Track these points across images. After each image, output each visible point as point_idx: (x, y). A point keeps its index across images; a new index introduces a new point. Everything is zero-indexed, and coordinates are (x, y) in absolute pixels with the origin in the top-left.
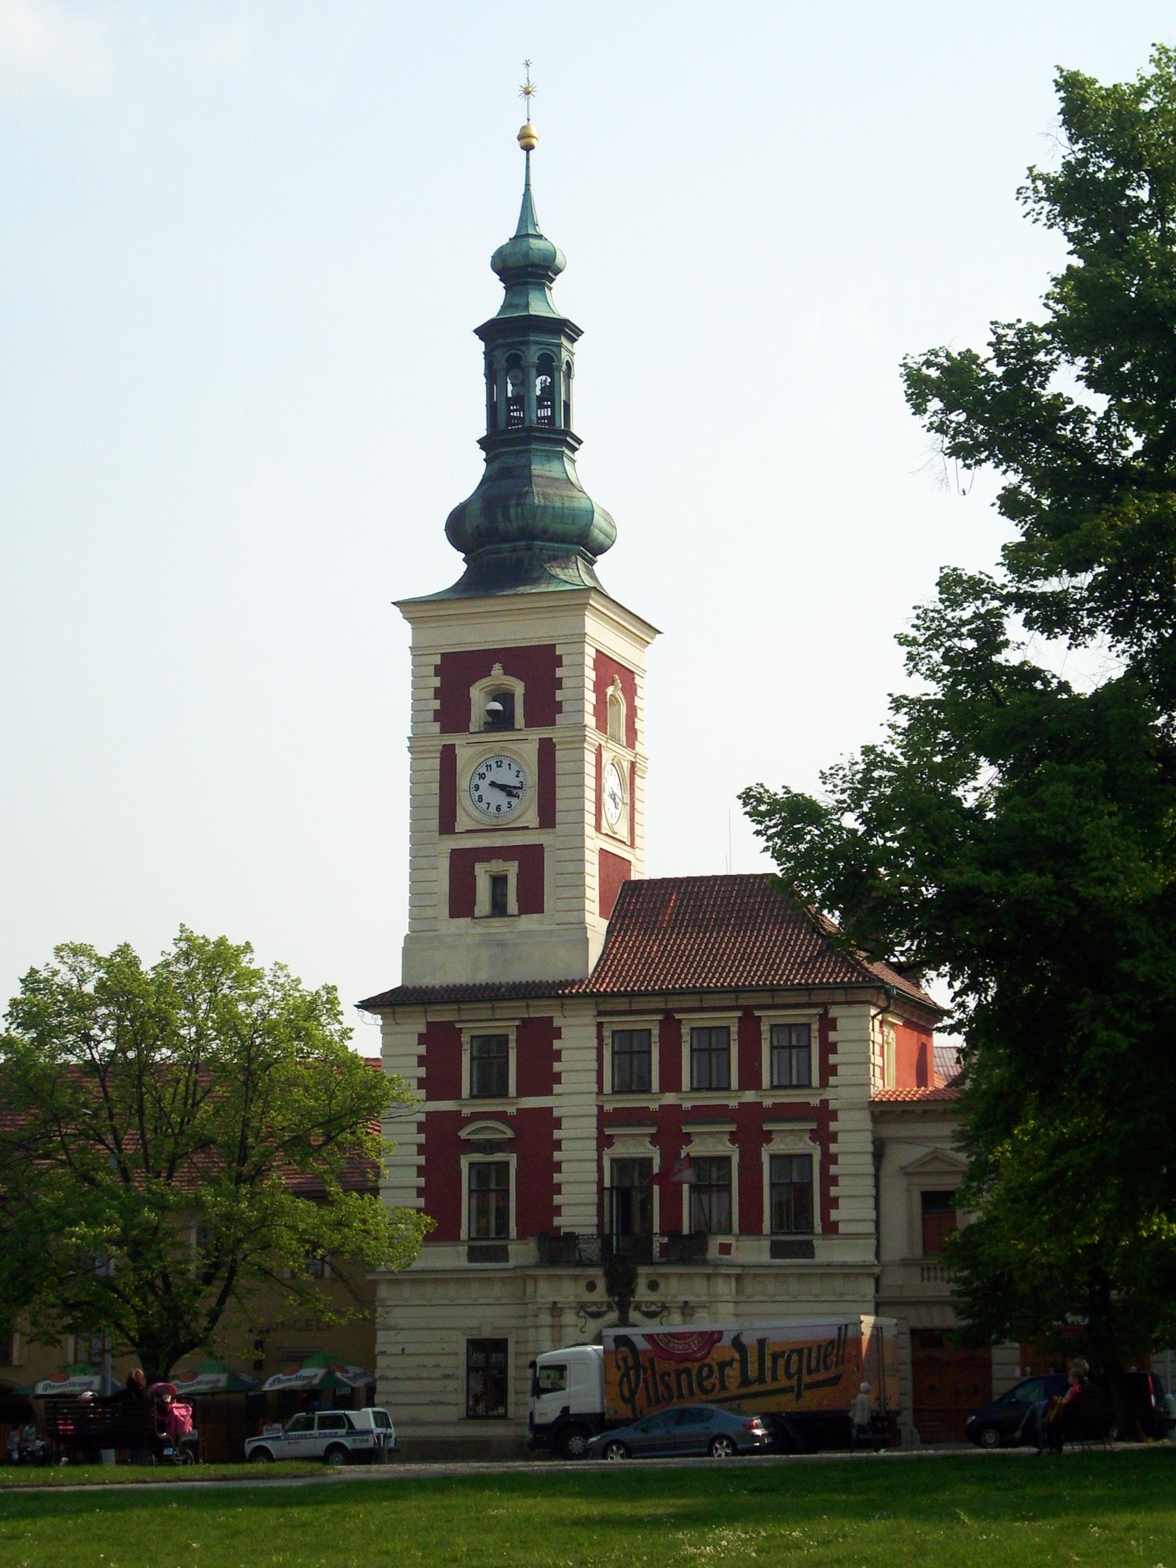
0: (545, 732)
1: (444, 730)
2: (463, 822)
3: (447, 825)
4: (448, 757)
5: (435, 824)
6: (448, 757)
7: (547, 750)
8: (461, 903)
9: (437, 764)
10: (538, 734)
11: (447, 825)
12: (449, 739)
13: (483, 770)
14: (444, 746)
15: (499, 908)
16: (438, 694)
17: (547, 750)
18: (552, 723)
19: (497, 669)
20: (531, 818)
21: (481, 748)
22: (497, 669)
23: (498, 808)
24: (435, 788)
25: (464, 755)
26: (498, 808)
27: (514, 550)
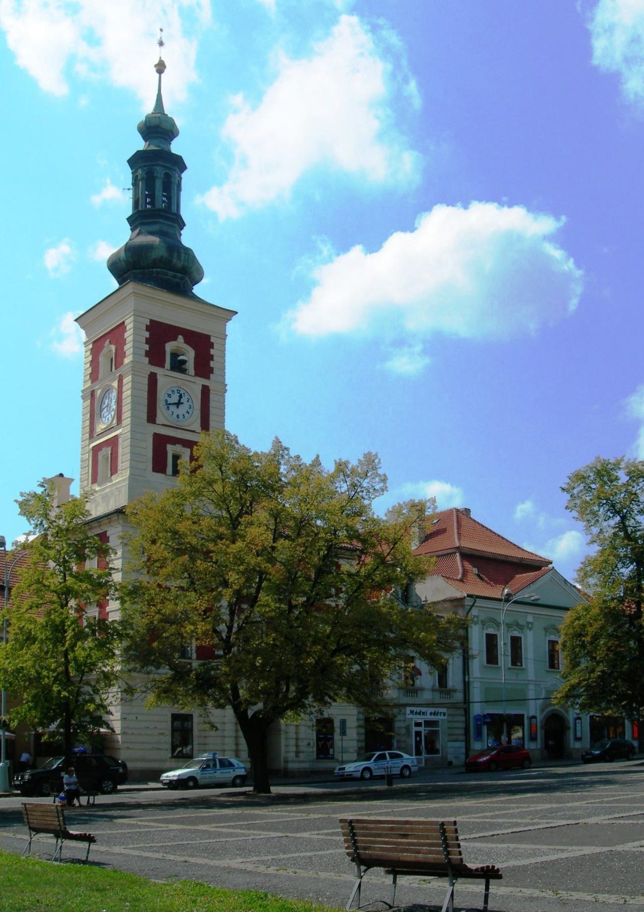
0: (205, 382)
1: (151, 363)
2: (160, 419)
3: (152, 417)
4: (153, 380)
5: (145, 416)
6: (153, 380)
7: (205, 392)
8: (159, 465)
9: (146, 381)
10: (202, 381)
11: (152, 417)
12: (155, 369)
13: (170, 393)
14: (151, 373)
15: (176, 472)
16: (148, 341)
17: (205, 392)
18: (208, 378)
19: (181, 338)
20: (197, 426)
21: (170, 379)
22: (181, 338)
23: (178, 416)
24: (145, 395)
25: (161, 381)
26: (178, 416)
27: (174, 277)
